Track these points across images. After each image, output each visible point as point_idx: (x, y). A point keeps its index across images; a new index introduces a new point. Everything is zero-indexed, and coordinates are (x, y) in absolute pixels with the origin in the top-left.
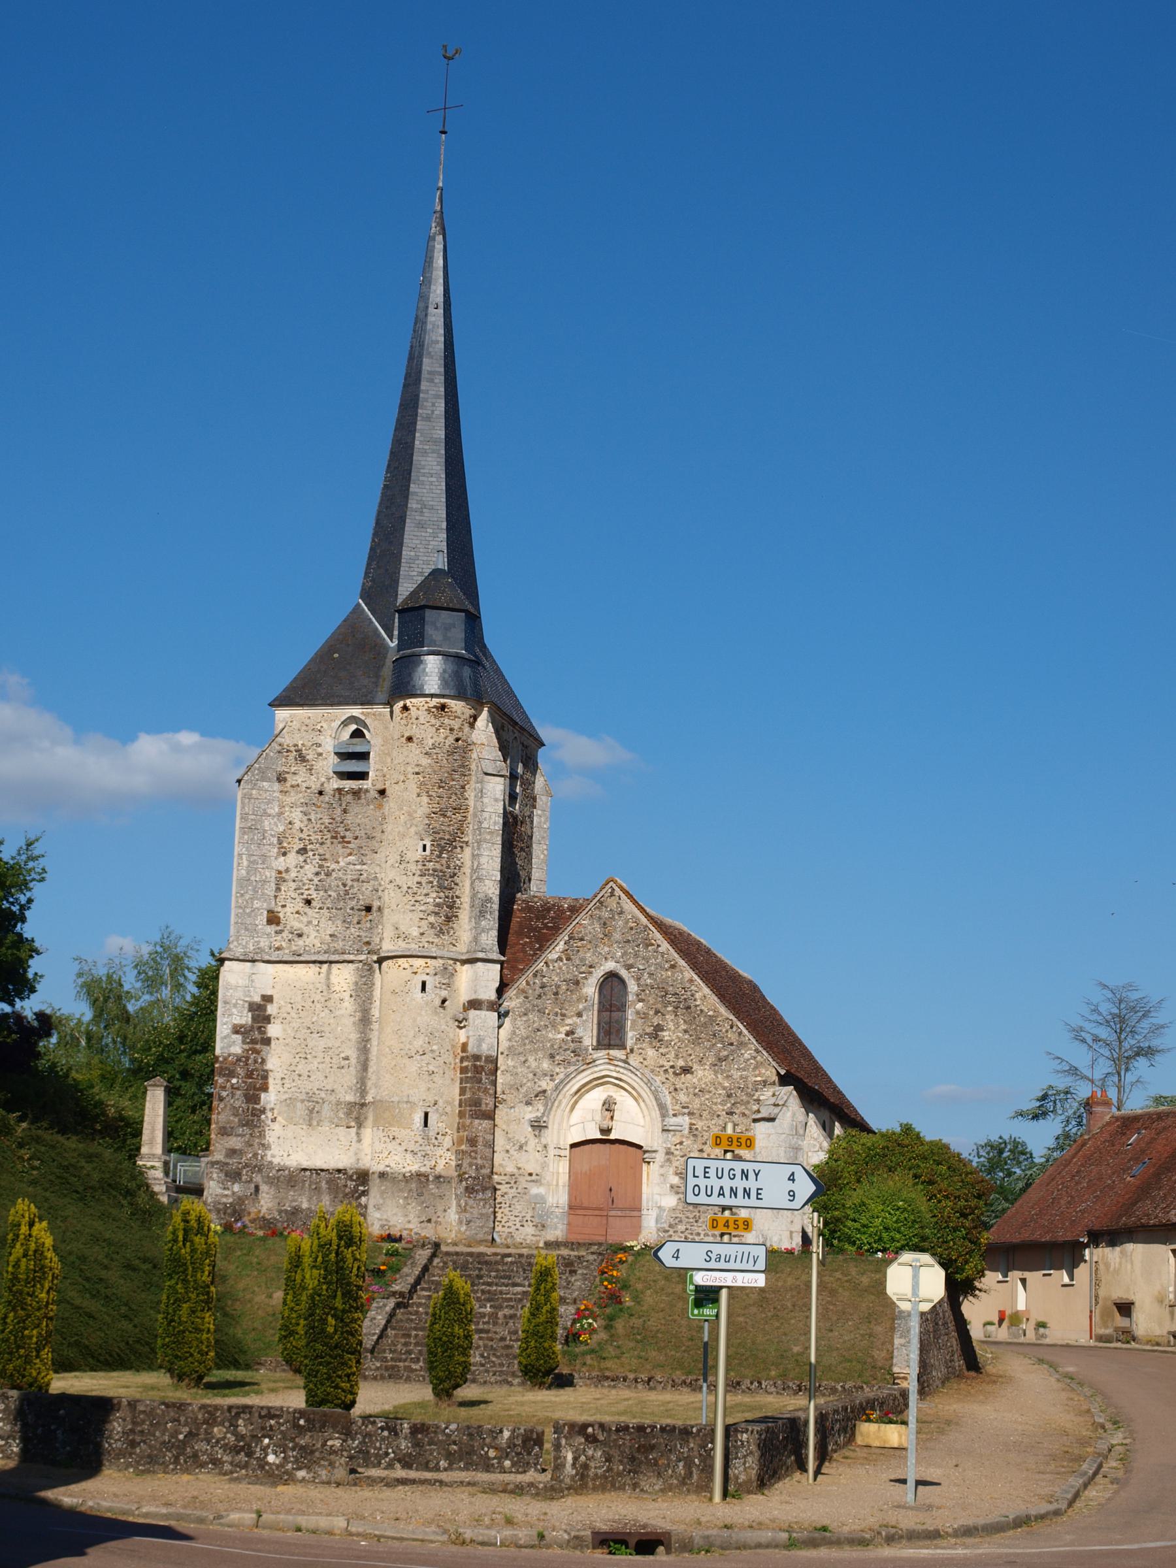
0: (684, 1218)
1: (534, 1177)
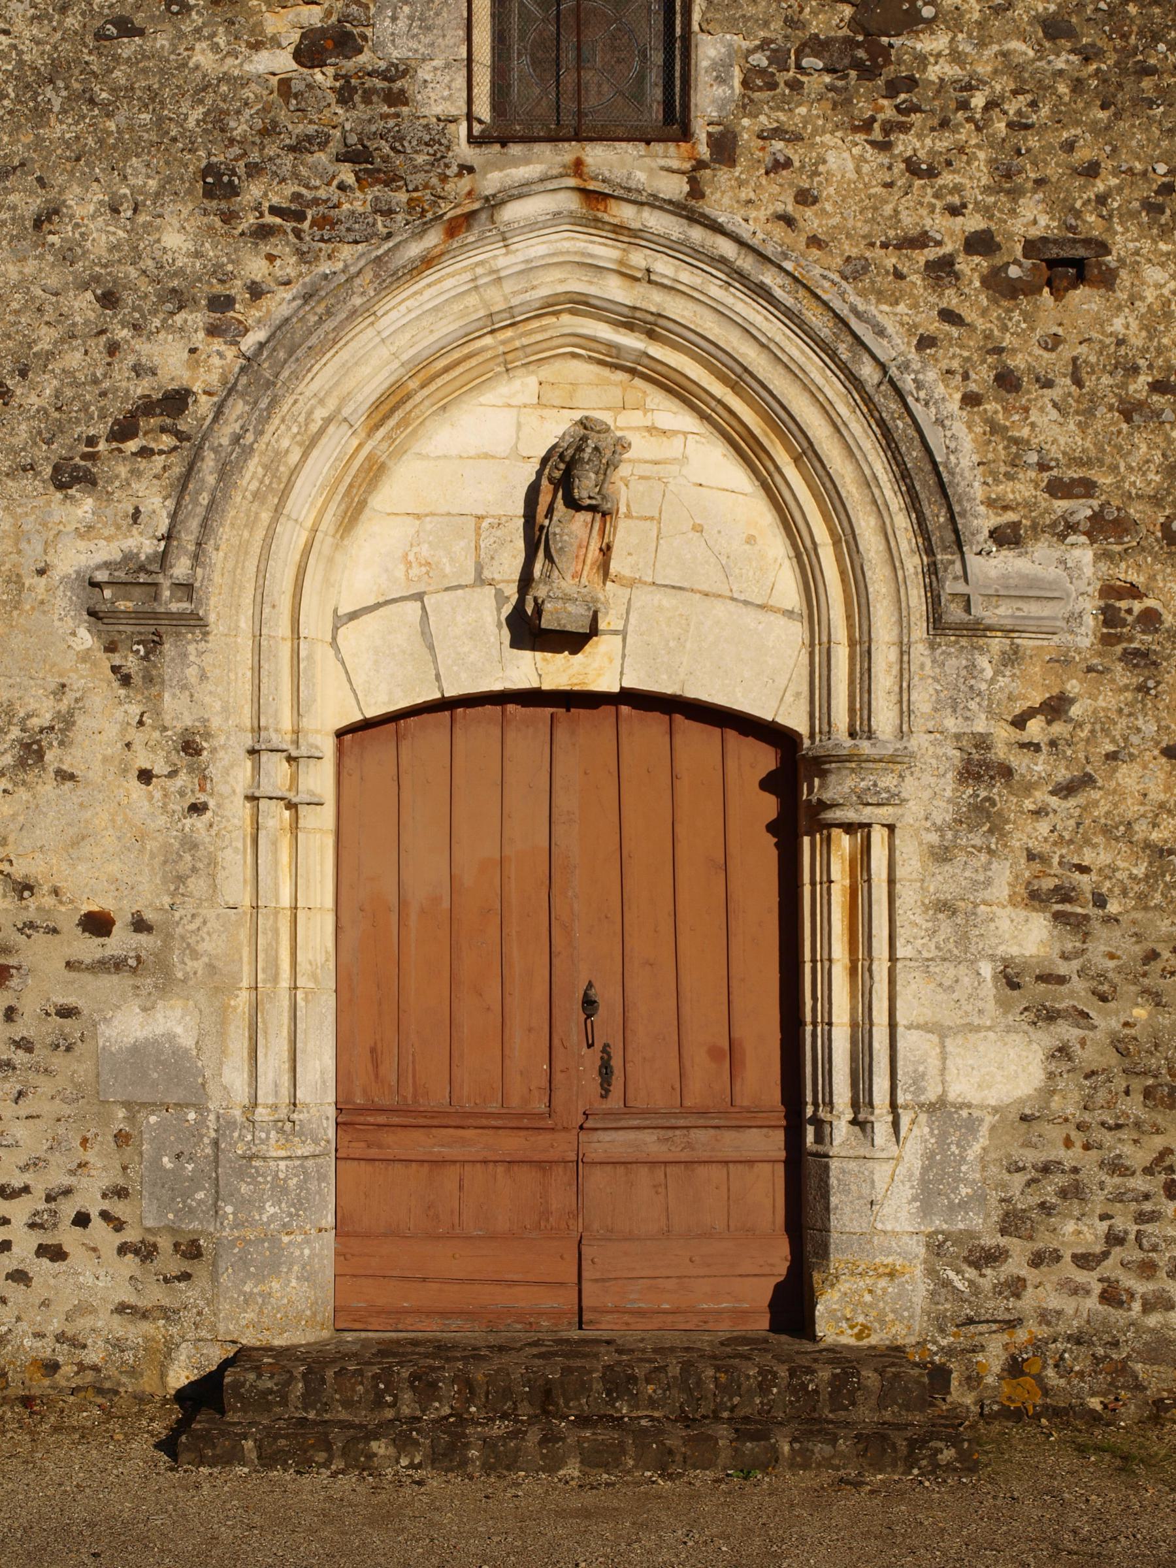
0: (1092, 1174)
1: (121, 941)
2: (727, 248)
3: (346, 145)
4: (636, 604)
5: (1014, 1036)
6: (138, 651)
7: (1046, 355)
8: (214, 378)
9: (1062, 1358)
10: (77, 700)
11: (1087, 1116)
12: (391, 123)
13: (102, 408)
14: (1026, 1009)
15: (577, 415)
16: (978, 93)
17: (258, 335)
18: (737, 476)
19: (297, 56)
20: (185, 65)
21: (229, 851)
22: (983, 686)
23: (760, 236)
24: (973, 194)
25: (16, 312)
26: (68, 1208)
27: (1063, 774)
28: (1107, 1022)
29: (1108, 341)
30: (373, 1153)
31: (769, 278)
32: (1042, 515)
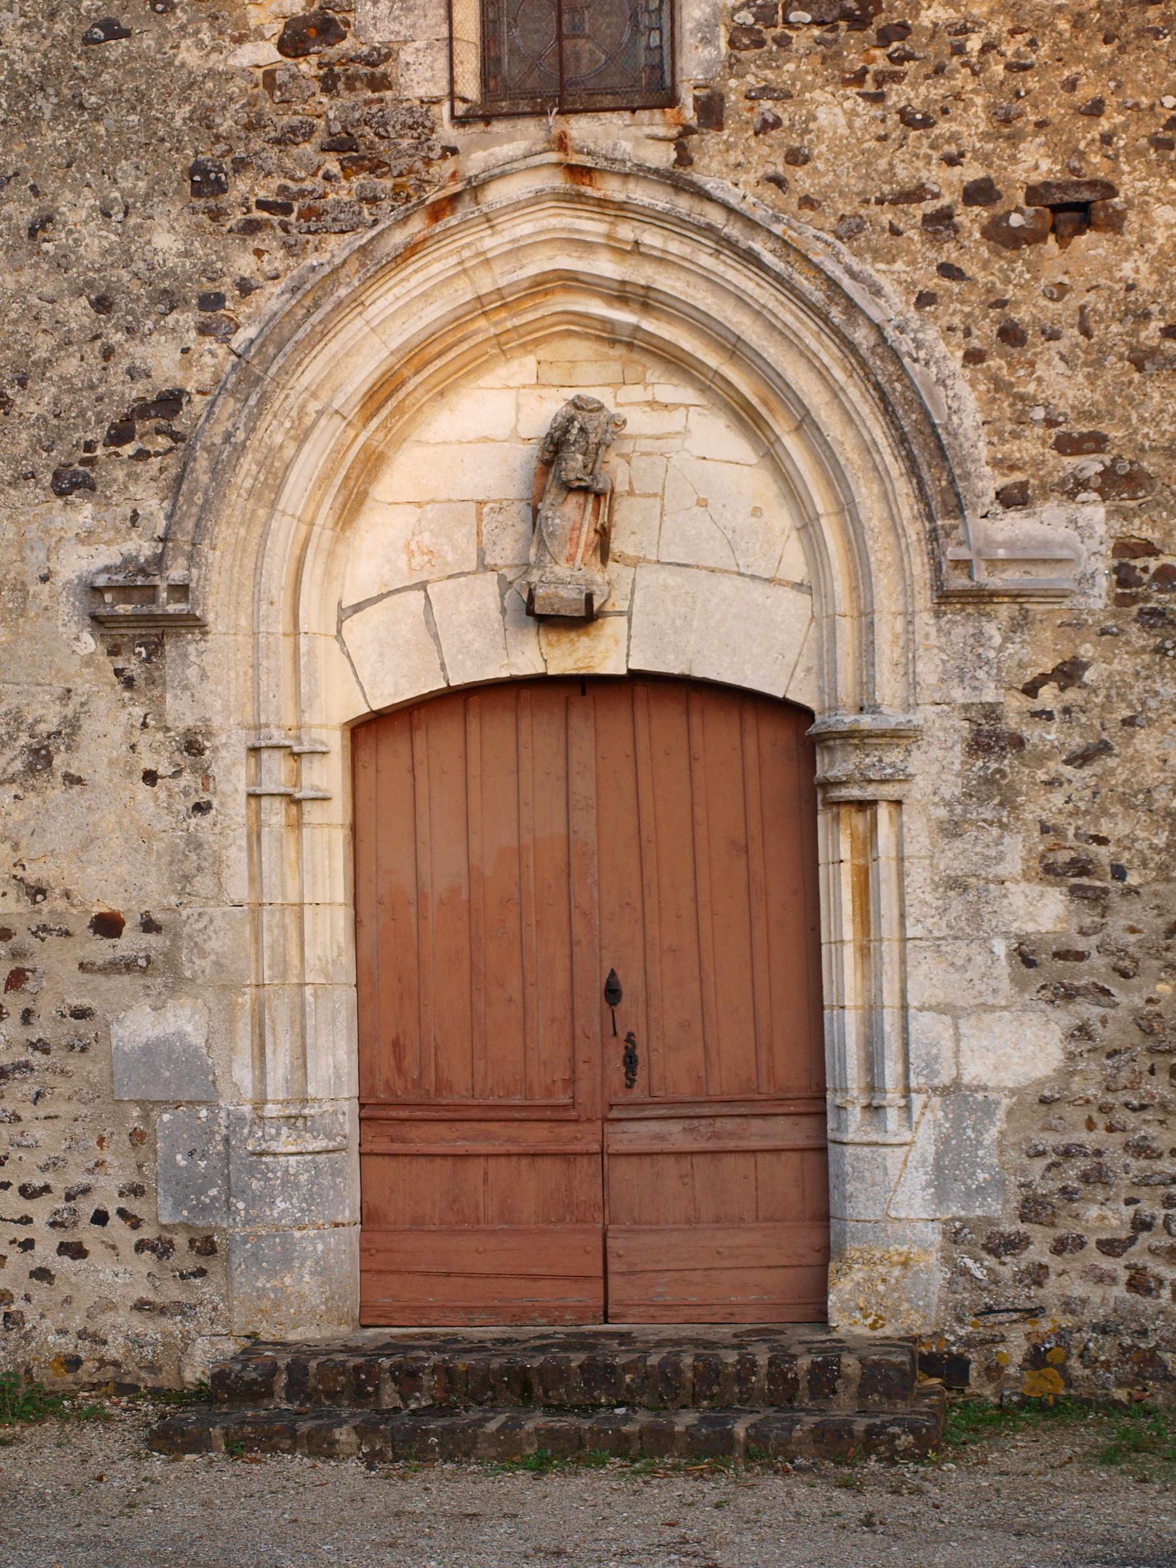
0: (1116, 1157)
1: (130, 942)
2: (715, 216)
3: (330, 134)
4: (640, 584)
5: (1032, 1016)
6: (140, 653)
7: (1051, 305)
8: (207, 377)
9: (1086, 1348)
10: (82, 704)
11: (1110, 1098)
12: (375, 108)
13: (99, 413)
14: (1043, 987)
15: (570, 394)
16: (973, 36)
17: (247, 333)
18: (738, 447)
19: (282, 47)
20: (171, 64)
21: (233, 849)
22: (992, 654)
23: (751, 199)
24: (971, 141)
25: (15, 322)
26: (87, 1208)
27: (1077, 742)
28: (1128, 999)
29: (1117, 287)
30: (396, 1147)
31: (758, 245)
32: (1050, 473)
